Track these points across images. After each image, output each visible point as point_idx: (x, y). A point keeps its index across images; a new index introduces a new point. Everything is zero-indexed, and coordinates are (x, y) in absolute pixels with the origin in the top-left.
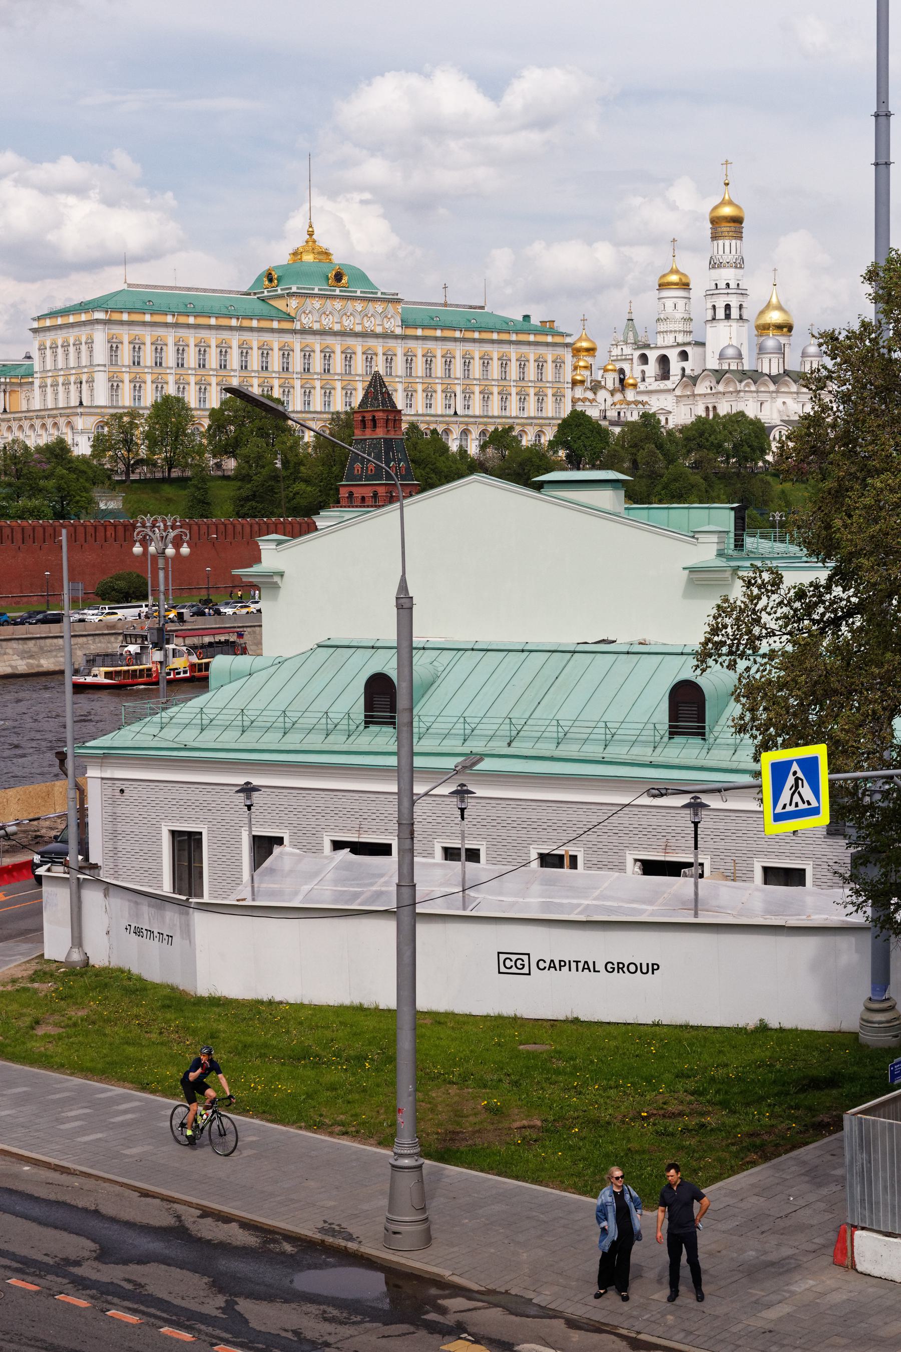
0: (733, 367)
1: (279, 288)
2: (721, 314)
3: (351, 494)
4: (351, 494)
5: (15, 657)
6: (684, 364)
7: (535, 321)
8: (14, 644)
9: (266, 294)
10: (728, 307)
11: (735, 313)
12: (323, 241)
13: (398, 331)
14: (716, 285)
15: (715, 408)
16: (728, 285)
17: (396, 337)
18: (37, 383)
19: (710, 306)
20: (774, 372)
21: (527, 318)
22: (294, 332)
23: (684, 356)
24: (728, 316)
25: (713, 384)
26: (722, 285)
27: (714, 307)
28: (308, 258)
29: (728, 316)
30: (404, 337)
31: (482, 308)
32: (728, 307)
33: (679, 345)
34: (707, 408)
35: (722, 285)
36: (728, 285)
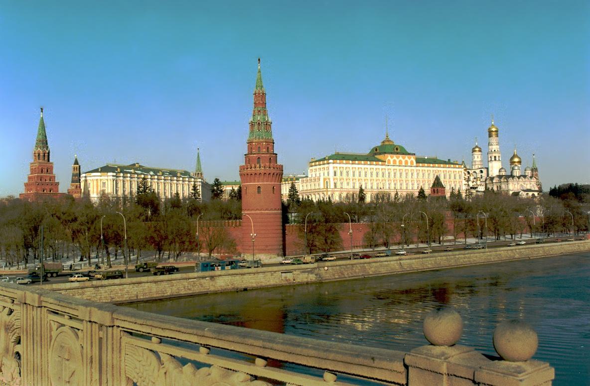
0: (504, 174)
2: (493, 159)
6: (482, 174)
10: (495, 157)
11: (497, 159)
12: (390, 138)
16: (495, 151)
20: (518, 175)
23: (482, 172)
24: (495, 160)
26: (493, 150)
32: (495, 157)
33: (479, 168)
34: (497, 187)
35: (493, 150)
36: (495, 151)
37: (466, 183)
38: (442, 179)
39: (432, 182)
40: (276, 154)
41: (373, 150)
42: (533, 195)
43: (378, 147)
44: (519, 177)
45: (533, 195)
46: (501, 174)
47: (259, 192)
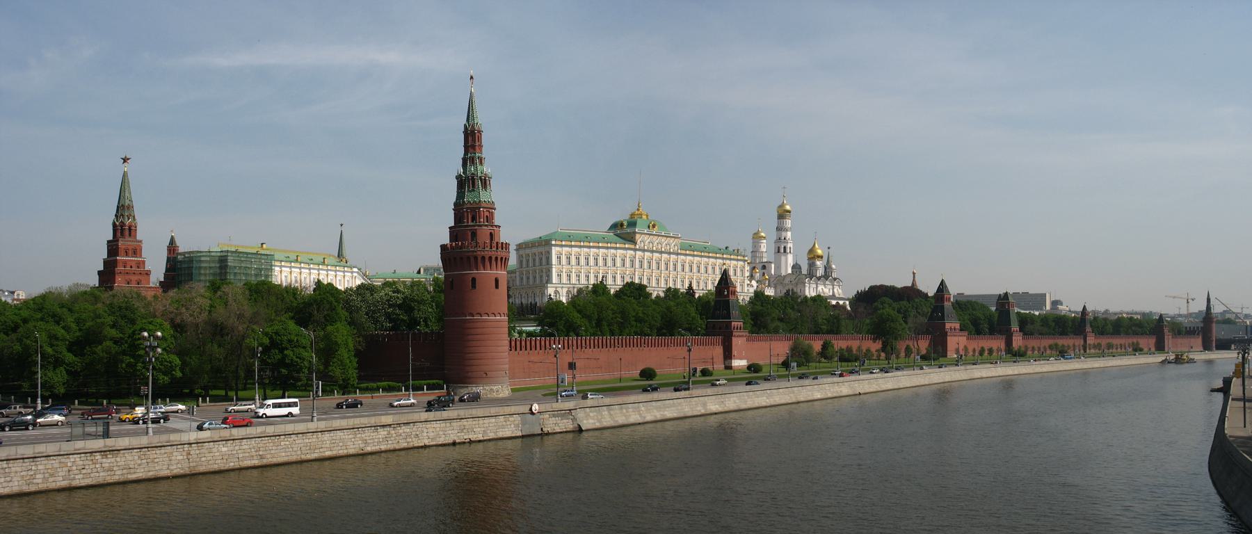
2: (782, 250)
3: (714, 325)
4: (714, 325)
5: (655, 411)
7: (731, 249)
8: (654, 403)
13: (679, 251)
14: (780, 239)
15: (792, 290)
17: (678, 254)
18: (518, 273)
19: (777, 246)
20: (818, 275)
22: (635, 250)
27: (779, 247)
29: (785, 251)
30: (681, 254)
32: (785, 248)
37: (749, 282)
38: (731, 273)
39: (718, 279)
40: (499, 227)
45: (837, 302)
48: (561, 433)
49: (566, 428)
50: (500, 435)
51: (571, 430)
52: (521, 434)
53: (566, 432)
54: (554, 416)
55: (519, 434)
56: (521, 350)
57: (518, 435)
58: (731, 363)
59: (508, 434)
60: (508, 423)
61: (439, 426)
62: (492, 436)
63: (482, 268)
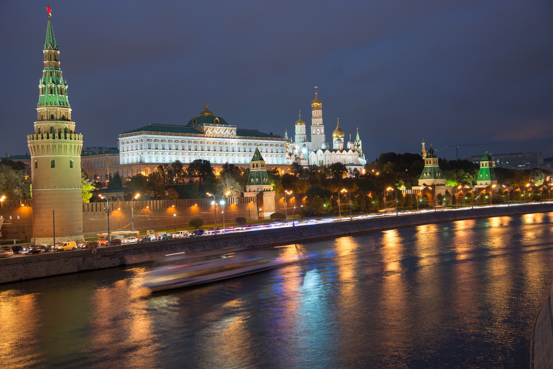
1: (199, 125)
7: (274, 134)
9: (194, 125)
21: (271, 133)
25: (322, 152)
28: (206, 114)
31: (258, 131)
33: (303, 142)
41: (191, 120)
42: (356, 170)
43: (196, 118)
44: (341, 151)
45: (356, 170)
46: (324, 148)
47: (53, 166)
48: (110, 268)
49: (114, 264)
50: (62, 272)
51: (118, 265)
52: (77, 271)
53: (114, 267)
54: (105, 256)
55: (77, 270)
56: (97, 211)
57: (75, 271)
58: (263, 215)
59: (68, 271)
60: (67, 263)
61: (7, 268)
62: (54, 273)
63: (52, 152)
